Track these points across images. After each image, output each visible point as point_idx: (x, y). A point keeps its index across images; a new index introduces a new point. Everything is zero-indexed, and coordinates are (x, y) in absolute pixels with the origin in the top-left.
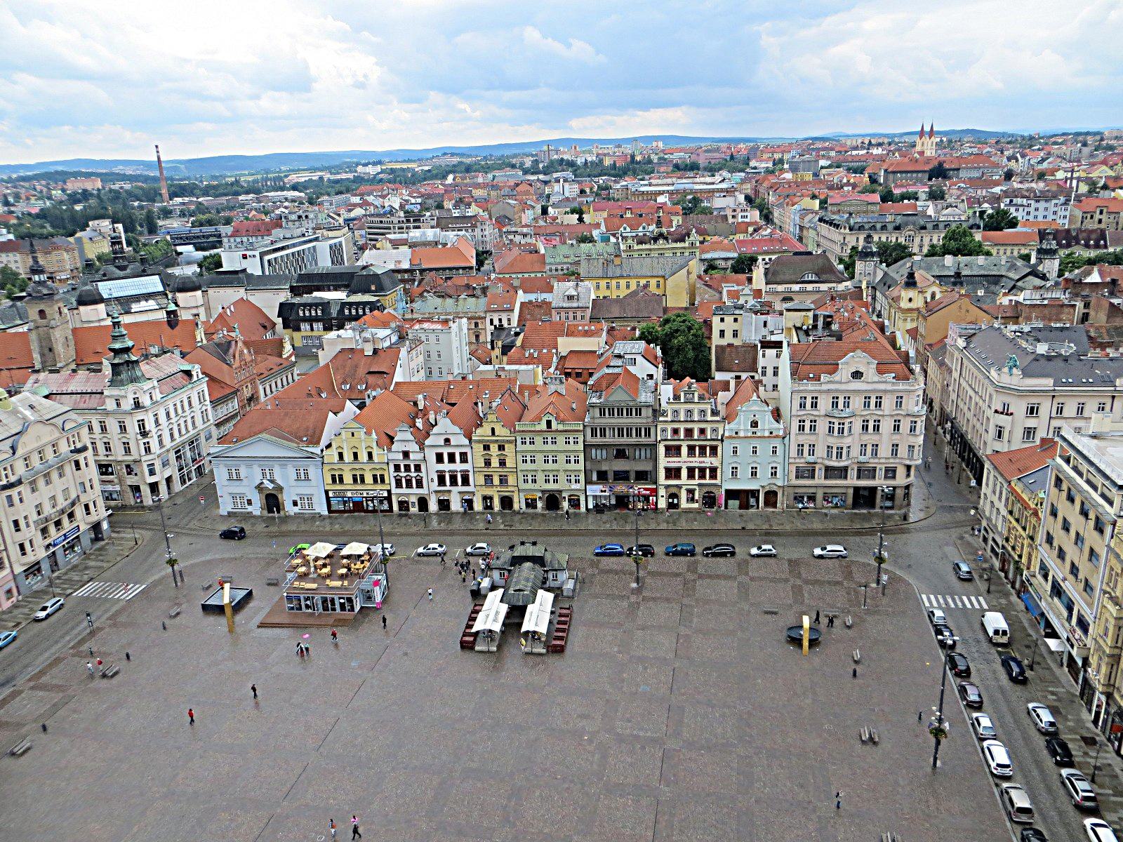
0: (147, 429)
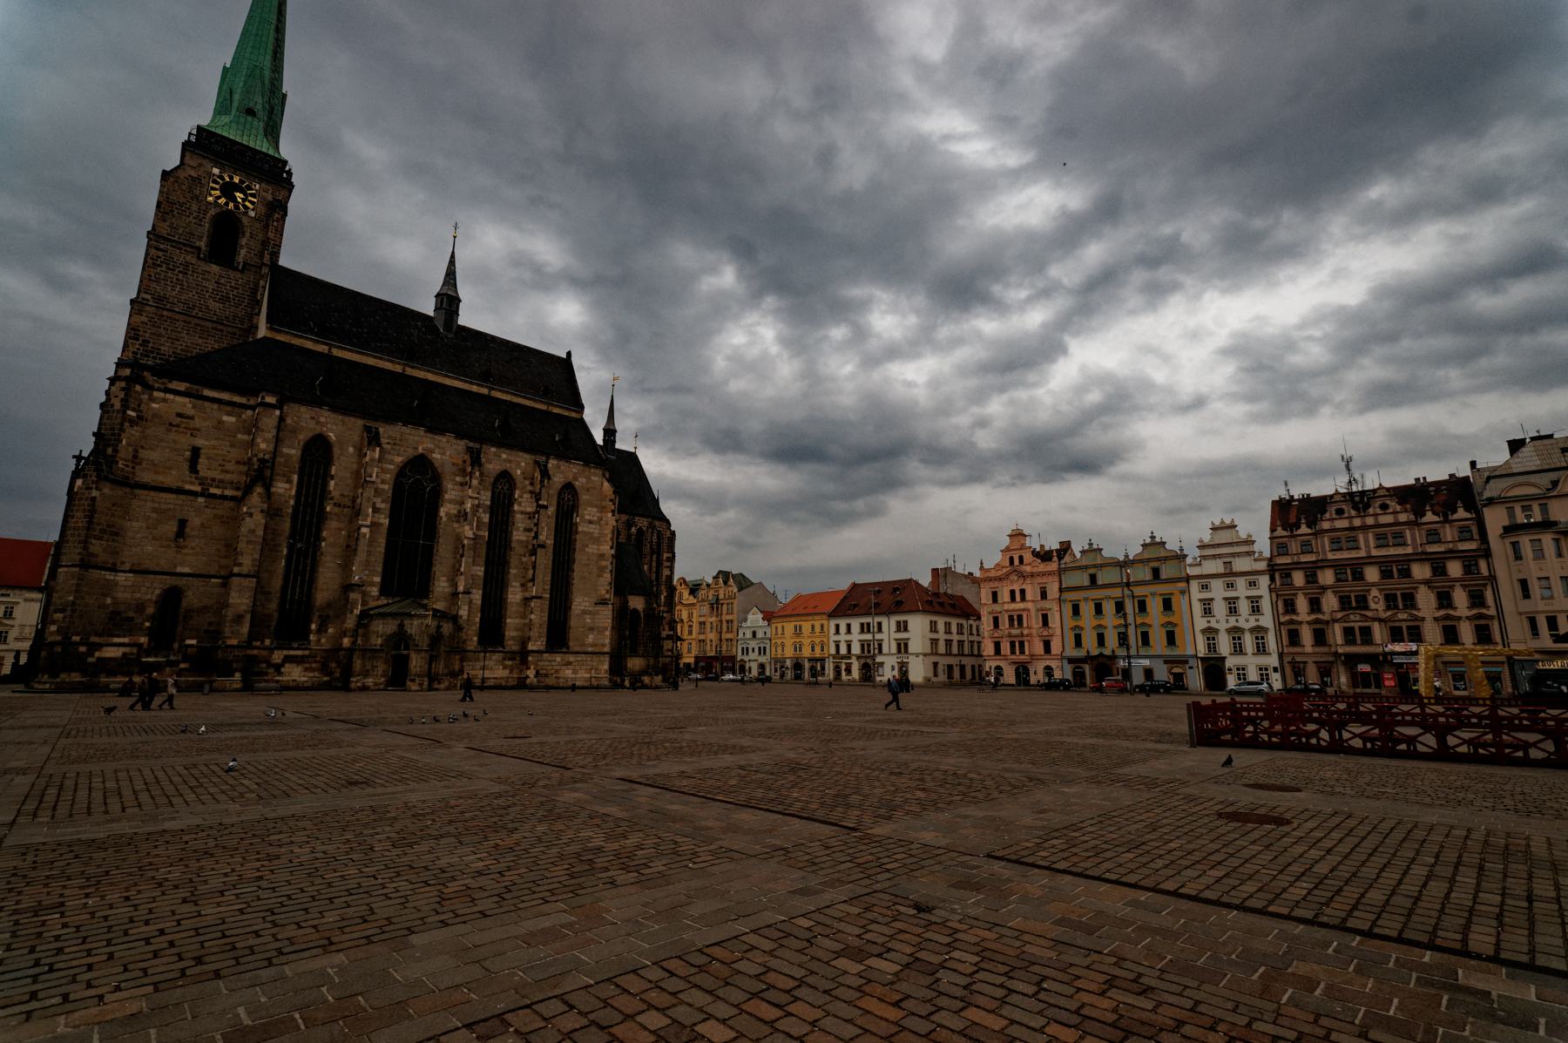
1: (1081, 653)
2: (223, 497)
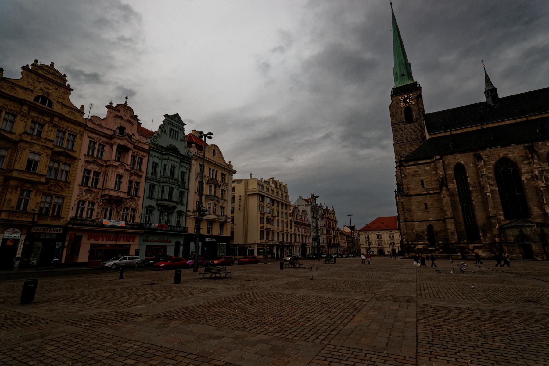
2: (434, 193)
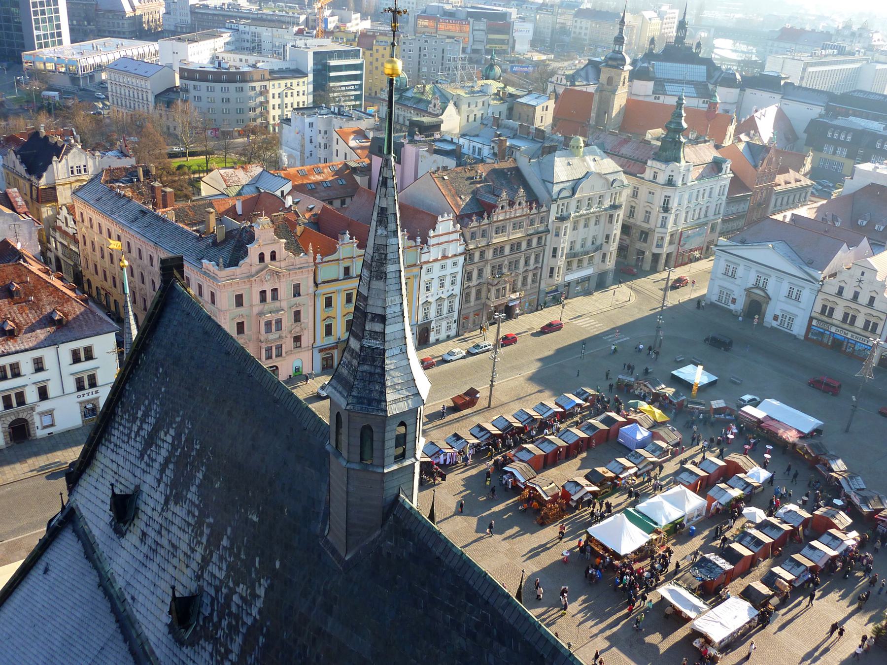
0: (670, 206)
1: (331, 340)
